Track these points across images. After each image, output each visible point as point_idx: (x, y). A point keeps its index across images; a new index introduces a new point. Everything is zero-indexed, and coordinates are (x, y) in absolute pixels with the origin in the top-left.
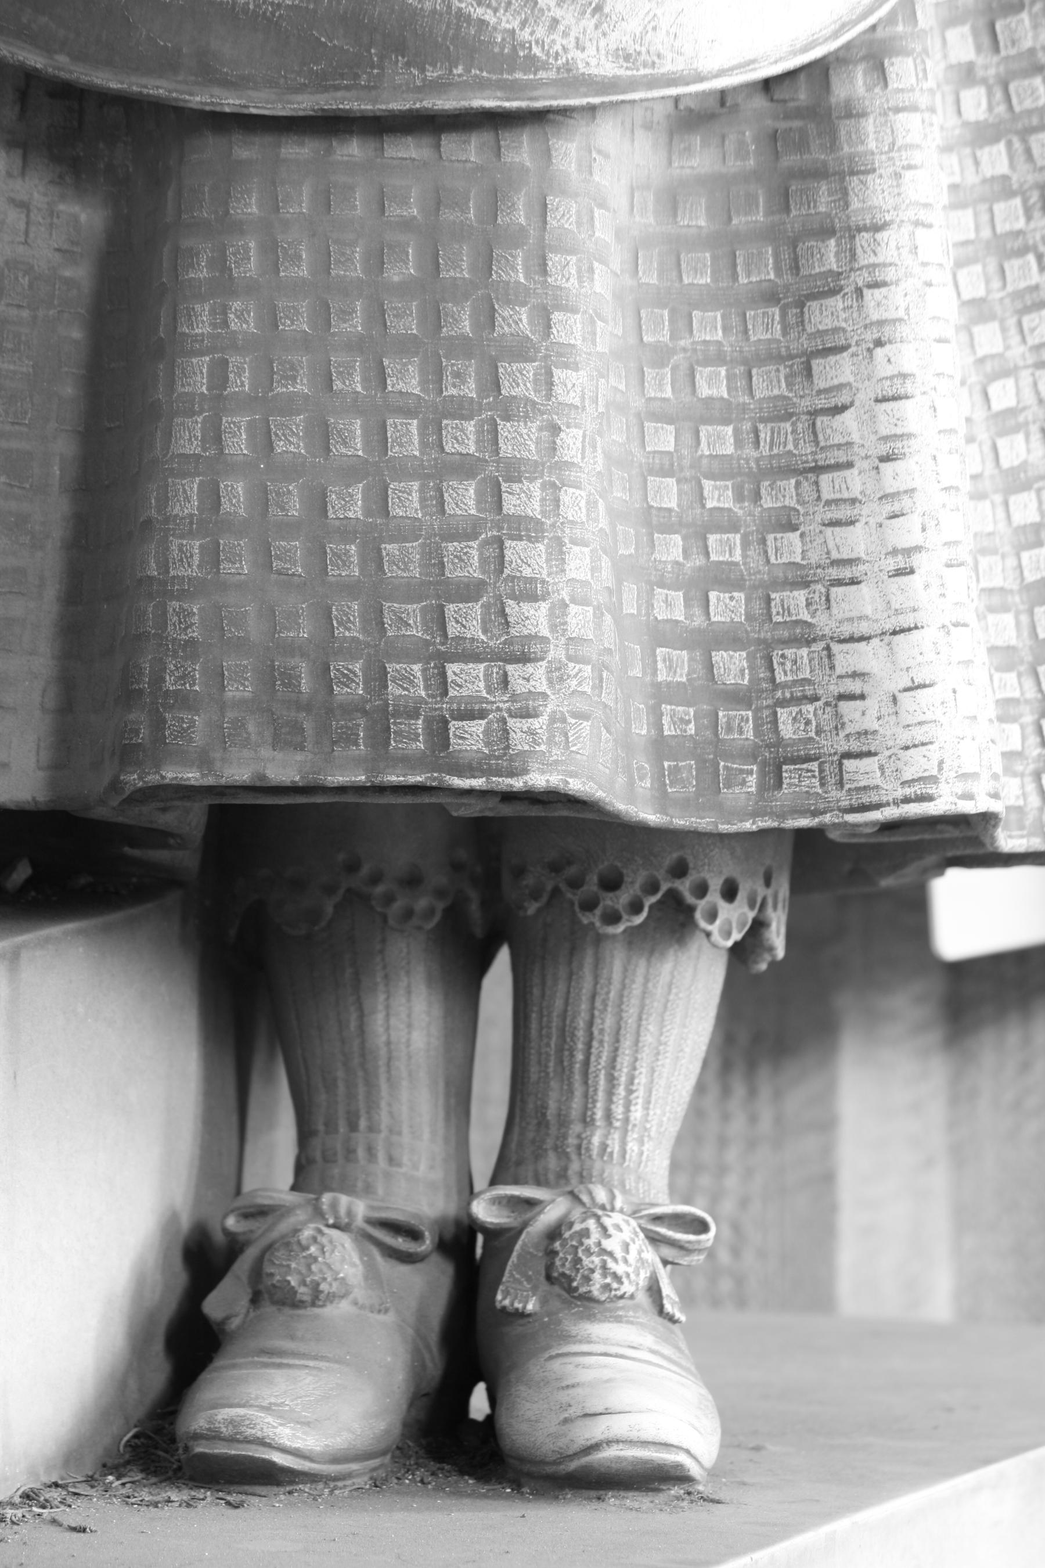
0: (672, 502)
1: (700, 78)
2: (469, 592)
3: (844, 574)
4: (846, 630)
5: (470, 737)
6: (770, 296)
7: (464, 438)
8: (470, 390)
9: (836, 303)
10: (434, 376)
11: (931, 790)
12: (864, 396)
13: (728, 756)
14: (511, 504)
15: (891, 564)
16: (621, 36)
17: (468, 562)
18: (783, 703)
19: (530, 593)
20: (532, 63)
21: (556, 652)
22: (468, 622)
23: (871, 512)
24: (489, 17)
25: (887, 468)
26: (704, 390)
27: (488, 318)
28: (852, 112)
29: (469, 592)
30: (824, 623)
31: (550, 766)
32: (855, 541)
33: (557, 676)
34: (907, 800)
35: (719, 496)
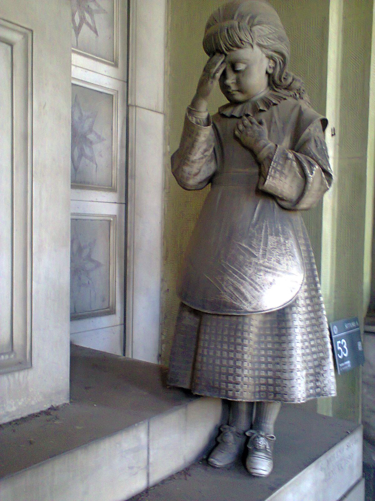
1: (264, 311)
2: (231, 375)
3: (284, 371)
4: (285, 378)
5: (230, 393)
6: (277, 335)
7: (232, 355)
8: (233, 349)
9: (285, 337)
10: (229, 346)
11: (294, 400)
12: (288, 349)
13: (270, 392)
14: (237, 364)
15: (290, 371)
17: (231, 371)
18: (277, 386)
19: (239, 376)
20: (241, 309)
21: (242, 383)
22: (231, 378)
23: (288, 364)
24: (236, 303)
25: (290, 359)
26: (268, 346)
27: (235, 340)
28: (288, 314)
29: (231, 375)
30: (282, 377)
31: (240, 398)
32: (286, 367)
33: (242, 387)
34: (291, 401)
35: (270, 360)
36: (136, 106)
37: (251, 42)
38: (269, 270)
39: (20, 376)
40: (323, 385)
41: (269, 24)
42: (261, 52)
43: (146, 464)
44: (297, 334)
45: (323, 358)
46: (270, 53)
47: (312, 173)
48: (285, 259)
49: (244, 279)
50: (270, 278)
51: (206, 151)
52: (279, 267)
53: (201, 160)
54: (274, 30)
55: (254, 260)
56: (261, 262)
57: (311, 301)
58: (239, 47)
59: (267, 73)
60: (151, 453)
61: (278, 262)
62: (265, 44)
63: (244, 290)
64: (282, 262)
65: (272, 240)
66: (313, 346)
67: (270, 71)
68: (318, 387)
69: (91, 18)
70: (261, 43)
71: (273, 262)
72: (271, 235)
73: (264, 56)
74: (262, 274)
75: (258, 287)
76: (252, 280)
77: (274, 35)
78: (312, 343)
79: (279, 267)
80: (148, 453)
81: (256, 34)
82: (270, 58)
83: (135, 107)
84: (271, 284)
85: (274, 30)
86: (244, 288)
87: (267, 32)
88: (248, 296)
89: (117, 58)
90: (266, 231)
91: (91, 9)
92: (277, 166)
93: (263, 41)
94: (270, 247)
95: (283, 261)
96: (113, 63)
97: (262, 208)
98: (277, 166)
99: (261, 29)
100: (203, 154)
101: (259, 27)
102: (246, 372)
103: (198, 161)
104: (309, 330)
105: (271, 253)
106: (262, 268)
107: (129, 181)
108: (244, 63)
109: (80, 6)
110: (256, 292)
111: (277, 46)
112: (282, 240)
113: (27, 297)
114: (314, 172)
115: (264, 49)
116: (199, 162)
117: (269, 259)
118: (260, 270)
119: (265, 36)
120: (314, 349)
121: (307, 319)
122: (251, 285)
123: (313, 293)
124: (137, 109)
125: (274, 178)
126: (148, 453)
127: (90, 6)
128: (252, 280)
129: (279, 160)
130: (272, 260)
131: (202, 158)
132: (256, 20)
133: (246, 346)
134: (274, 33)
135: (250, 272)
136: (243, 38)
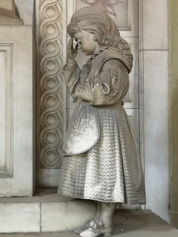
0: (81, 179)
16: (70, 151)
36: (143, 50)
37: (78, 29)
38: (79, 135)
39: (8, 180)
40: (113, 196)
41: (84, 19)
42: (86, 32)
43: (39, 221)
44: (90, 166)
45: (115, 182)
46: (91, 31)
47: (93, 88)
48: (87, 129)
49: (69, 139)
50: (79, 138)
51: (74, 81)
52: (84, 133)
53: (71, 86)
54: (89, 21)
55: (74, 130)
56: (77, 131)
57: (112, 152)
58: (75, 33)
59: (94, 40)
60: (42, 217)
61: (84, 131)
62: (86, 28)
63: (68, 144)
64: (85, 131)
65: (83, 120)
66: (112, 175)
67: (95, 39)
68: (111, 197)
69: (112, 9)
70: (84, 28)
71: (82, 131)
72: (83, 118)
73: (89, 33)
74: (76, 136)
75: (73, 143)
76: (72, 139)
77: (89, 23)
78: (112, 174)
79: (84, 133)
80: (41, 217)
81: (80, 25)
82: (93, 33)
83: (142, 51)
84: (79, 141)
85: (89, 21)
86: (69, 143)
87: (85, 23)
88: (69, 147)
89: (131, 25)
90: (81, 117)
91: (112, 4)
92: (81, 86)
93: (84, 28)
94: (81, 124)
95: (86, 130)
96: (128, 29)
97: (83, 106)
98: (81, 86)
99: (81, 23)
100: (72, 83)
101: (80, 22)
102: (67, 182)
103: (70, 86)
104: (110, 167)
105: (81, 127)
106: (77, 134)
107: (140, 94)
108: (80, 39)
109: (104, 5)
110: (72, 145)
111: (91, 28)
112: (88, 120)
113: (12, 148)
114: (95, 87)
115: (87, 31)
116: (71, 87)
117: (80, 130)
118: (76, 135)
119: (84, 25)
120: (112, 177)
121: (110, 161)
122: (71, 142)
123: (113, 148)
124: (144, 51)
125: (80, 91)
126: (41, 217)
127: (111, 2)
128: (72, 139)
129: (83, 83)
130: (81, 130)
131: (72, 85)
132: (77, 20)
133: (68, 170)
134: (88, 22)
135: (72, 136)
136: (74, 29)
